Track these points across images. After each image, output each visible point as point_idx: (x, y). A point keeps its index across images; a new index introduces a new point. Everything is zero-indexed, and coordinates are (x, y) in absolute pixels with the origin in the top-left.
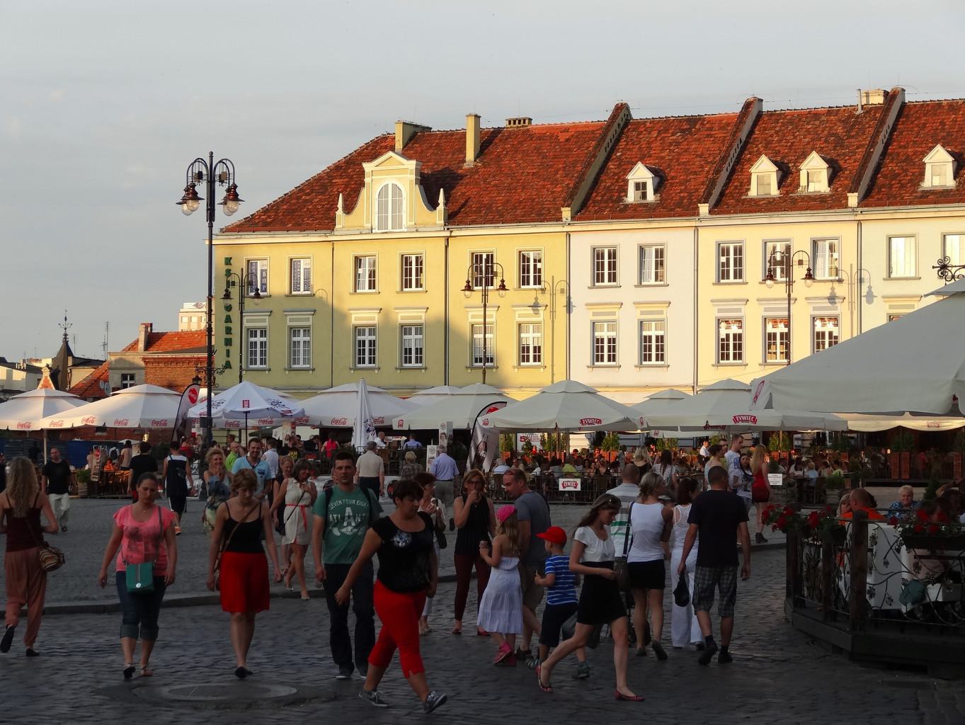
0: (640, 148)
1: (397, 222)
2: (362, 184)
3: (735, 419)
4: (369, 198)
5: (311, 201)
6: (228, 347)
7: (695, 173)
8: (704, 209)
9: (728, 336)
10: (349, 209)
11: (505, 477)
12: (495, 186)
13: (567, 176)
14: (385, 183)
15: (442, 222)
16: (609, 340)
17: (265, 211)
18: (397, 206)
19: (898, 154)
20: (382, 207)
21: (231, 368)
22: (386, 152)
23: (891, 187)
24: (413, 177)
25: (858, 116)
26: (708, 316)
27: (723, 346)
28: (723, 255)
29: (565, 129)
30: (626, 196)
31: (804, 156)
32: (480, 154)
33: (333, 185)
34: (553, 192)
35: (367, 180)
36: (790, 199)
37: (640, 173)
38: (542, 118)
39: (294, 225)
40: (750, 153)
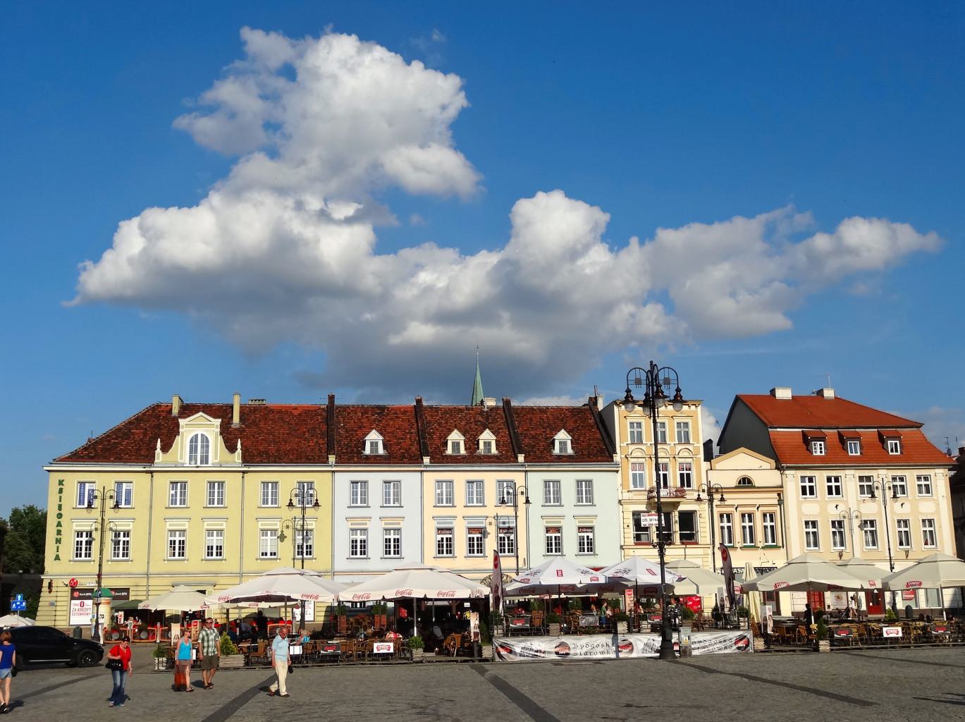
0: (354, 422)
1: (205, 460)
2: (178, 433)
4: (182, 443)
6: (58, 544)
8: (426, 460)
9: (442, 539)
10: (166, 449)
11: (458, 637)
12: (262, 440)
13: (313, 436)
14: (194, 434)
15: (240, 461)
16: (361, 541)
17: (85, 449)
19: (526, 434)
20: (193, 449)
21: (59, 560)
22: (198, 412)
23: (535, 452)
24: (218, 430)
27: (440, 545)
28: (439, 489)
29: (296, 408)
30: (364, 450)
33: (133, 434)
34: (309, 446)
35: (181, 430)
36: (473, 458)
37: (374, 436)
40: (432, 429)
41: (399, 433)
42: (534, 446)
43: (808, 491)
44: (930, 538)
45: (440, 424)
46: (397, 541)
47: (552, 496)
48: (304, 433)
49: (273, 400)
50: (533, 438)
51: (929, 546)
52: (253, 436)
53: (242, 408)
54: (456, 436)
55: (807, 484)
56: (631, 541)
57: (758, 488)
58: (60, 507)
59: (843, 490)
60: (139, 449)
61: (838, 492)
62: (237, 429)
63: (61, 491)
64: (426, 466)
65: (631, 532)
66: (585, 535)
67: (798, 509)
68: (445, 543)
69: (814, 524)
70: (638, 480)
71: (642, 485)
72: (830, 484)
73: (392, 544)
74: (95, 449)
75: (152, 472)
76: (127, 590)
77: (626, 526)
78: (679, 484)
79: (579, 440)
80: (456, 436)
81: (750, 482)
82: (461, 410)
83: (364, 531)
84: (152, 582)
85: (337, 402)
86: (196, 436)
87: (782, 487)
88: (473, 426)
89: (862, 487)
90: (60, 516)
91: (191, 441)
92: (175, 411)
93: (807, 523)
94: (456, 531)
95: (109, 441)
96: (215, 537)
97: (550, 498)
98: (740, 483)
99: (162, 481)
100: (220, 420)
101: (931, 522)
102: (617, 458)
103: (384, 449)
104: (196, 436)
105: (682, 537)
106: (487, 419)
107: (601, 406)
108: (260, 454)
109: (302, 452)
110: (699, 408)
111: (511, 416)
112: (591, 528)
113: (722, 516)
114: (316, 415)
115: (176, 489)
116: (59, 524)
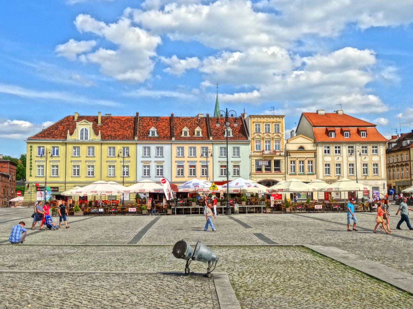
1: (86, 138)
3: (234, 191)
5: (54, 131)
7: (164, 130)
9: (179, 169)
10: (71, 134)
13: (129, 129)
15: (100, 139)
16: (147, 170)
17: (41, 133)
18: (86, 134)
20: (82, 134)
23: (217, 136)
25: (199, 119)
26: (175, 165)
27: (179, 172)
31: (184, 127)
32: (102, 122)
33: (59, 128)
35: (77, 126)
36: (192, 138)
37: (153, 129)
38: (112, 115)
39: (52, 138)
41: (164, 128)
42: (217, 133)
43: (327, 152)
44: (376, 171)
45: (180, 124)
46: (162, 170)
47: (223, 153)
48: (126, 128)
49: (114, 114)
50: (217, 130)
51: (376, 174)
52: (106, 129)
53: (102, 117)
54: (185, 129)
55: (327, 149)
56: (254, 171)
57: (307, 151)
58: (31, 156)
59: (341, 152)
60: (61, 134)
61: (339, 152)
62: (100, 126)
63: (31, 150)
64: (173, 141)
65: (254, 168)
66: (236, 168)
67: (322, 158)
68: (180, 171)
69: (329, 165)
70: (258, 147)
71: (259, 149)
72: (336, 149)
73: (160, 171)
74: (44, 134)
75: (66, 144)
76: (58, 188)
77: (252, 165)
78: (274, 149)
79: (235, 131)
80: (185, 129)
81: (303, 148)
82: (189, 119)
83: (149, 166)
84: (67, 185)
85: (140, 115)
86: (83, 129)
87: (316, 150)
88: (193, 125)
89: (349, 150)
90: (31, 159)
91: (81, 131)
92: (76, 119)
93: (326, 165)
94: (197, 167)
95: (50, 131)
96: (91, 168)
97: (235, 154)
98: (299, 148)
99: (70, 147)
100: (91, 124)
101: (377, 165)
102: (250, 138)
103: (157, 134)
104: (83, 129)
105: (275, 170)
106: (199, 122)
107: (246, 117)
108: (108, 136)
109: (125, 135)
110: (284, 119)
111: (209, 121)
112: (238, 166)
113: (291, 162)
114: (131, 120)
115: (76, 149)
116: (31, 163)
